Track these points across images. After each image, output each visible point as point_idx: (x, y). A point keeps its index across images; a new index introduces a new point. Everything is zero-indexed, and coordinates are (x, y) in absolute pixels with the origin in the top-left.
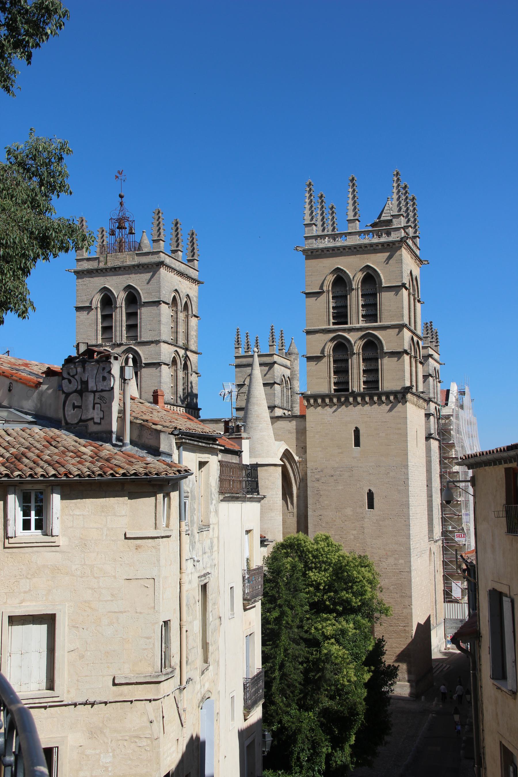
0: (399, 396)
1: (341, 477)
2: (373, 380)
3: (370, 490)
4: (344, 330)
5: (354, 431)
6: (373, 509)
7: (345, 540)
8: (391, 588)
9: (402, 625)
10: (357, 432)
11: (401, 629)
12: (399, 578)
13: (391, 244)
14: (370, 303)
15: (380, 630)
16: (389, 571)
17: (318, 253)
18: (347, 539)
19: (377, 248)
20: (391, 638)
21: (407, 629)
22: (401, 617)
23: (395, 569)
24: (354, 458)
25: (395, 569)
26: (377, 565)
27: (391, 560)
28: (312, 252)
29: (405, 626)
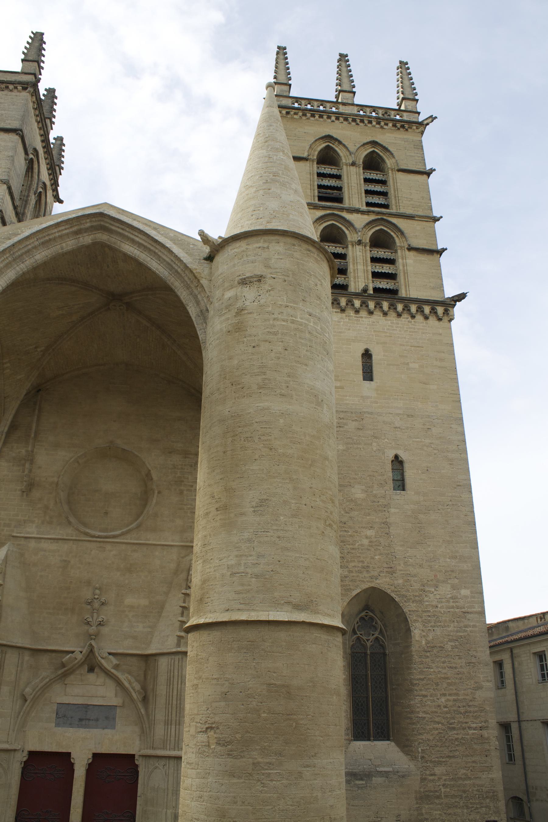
0: (440, 310)
1: (341, 429)
2: (388, 287)
3: (396, 457)
4: (342, 209)
5: (363, 355)
6: (404, 490)
7: (351, 546)
8: (448, 647)
9: (474, 725)
10: (367, 355)
11: (473, 734)
12: (462, 624)
13: (406, 126)
14: (376, 189)
15: (429, 740)
16: (442, 611)
17: (295, 116)
18: (356, 546)
19: (385, 127)
20: (454, 757)
21: (485, 733)
22: (472, 709)
23: (453, 607)
24: (362, 397)
25: (453, 607)
26: (417, 598)
27: (445, 590)
28: (288, 113)
29: (481, 728)
